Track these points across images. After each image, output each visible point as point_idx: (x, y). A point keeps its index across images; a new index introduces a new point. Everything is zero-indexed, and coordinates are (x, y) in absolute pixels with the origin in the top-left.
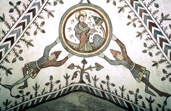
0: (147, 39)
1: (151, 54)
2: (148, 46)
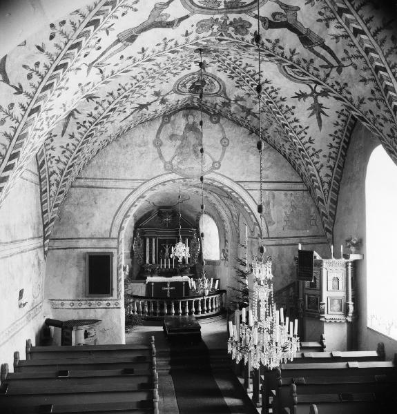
0: (72, 23)
1: (52, 37)
2: (62, 28)
